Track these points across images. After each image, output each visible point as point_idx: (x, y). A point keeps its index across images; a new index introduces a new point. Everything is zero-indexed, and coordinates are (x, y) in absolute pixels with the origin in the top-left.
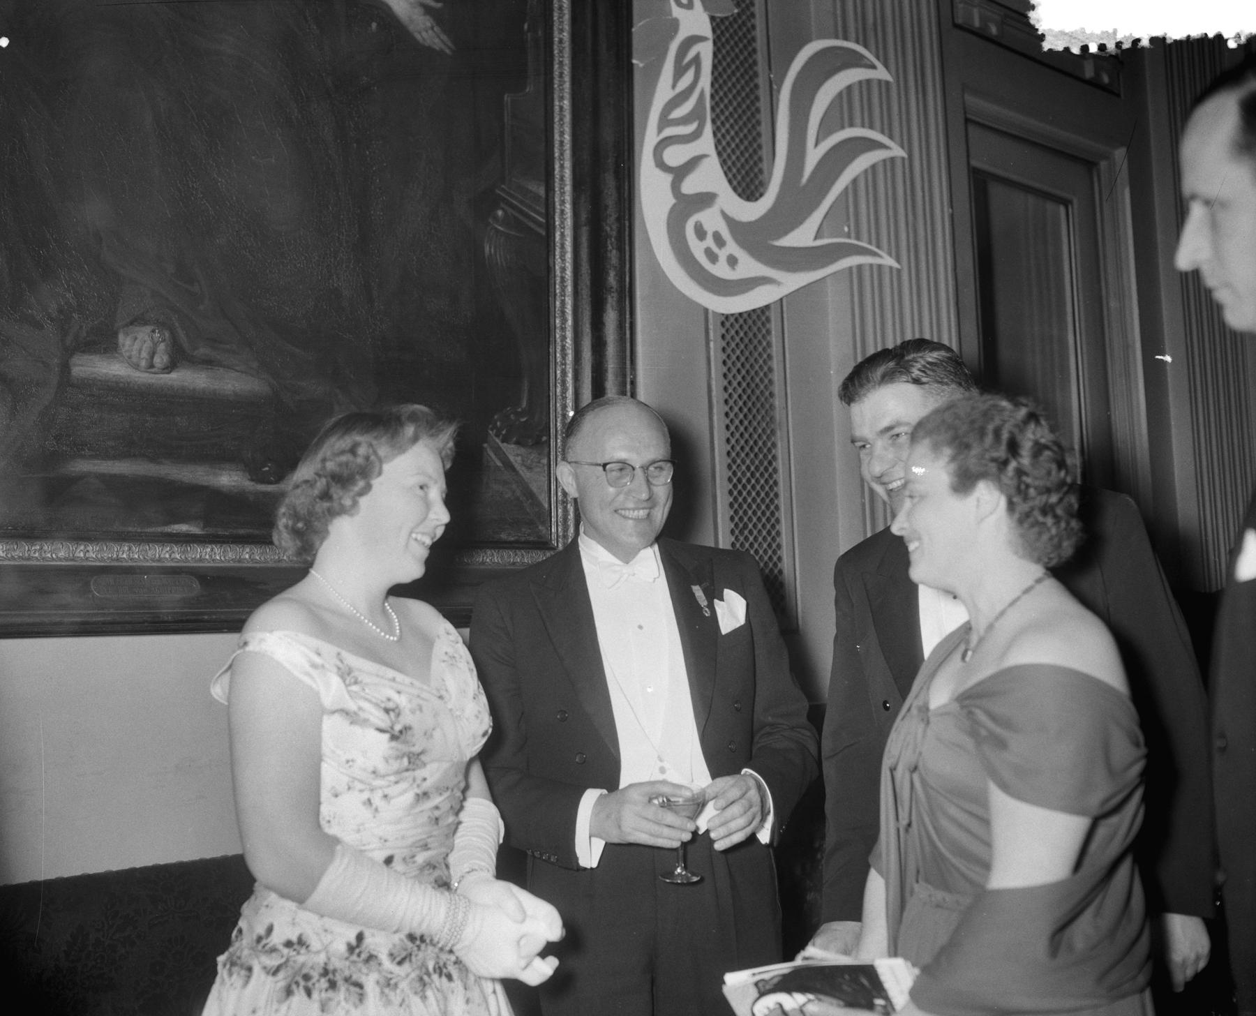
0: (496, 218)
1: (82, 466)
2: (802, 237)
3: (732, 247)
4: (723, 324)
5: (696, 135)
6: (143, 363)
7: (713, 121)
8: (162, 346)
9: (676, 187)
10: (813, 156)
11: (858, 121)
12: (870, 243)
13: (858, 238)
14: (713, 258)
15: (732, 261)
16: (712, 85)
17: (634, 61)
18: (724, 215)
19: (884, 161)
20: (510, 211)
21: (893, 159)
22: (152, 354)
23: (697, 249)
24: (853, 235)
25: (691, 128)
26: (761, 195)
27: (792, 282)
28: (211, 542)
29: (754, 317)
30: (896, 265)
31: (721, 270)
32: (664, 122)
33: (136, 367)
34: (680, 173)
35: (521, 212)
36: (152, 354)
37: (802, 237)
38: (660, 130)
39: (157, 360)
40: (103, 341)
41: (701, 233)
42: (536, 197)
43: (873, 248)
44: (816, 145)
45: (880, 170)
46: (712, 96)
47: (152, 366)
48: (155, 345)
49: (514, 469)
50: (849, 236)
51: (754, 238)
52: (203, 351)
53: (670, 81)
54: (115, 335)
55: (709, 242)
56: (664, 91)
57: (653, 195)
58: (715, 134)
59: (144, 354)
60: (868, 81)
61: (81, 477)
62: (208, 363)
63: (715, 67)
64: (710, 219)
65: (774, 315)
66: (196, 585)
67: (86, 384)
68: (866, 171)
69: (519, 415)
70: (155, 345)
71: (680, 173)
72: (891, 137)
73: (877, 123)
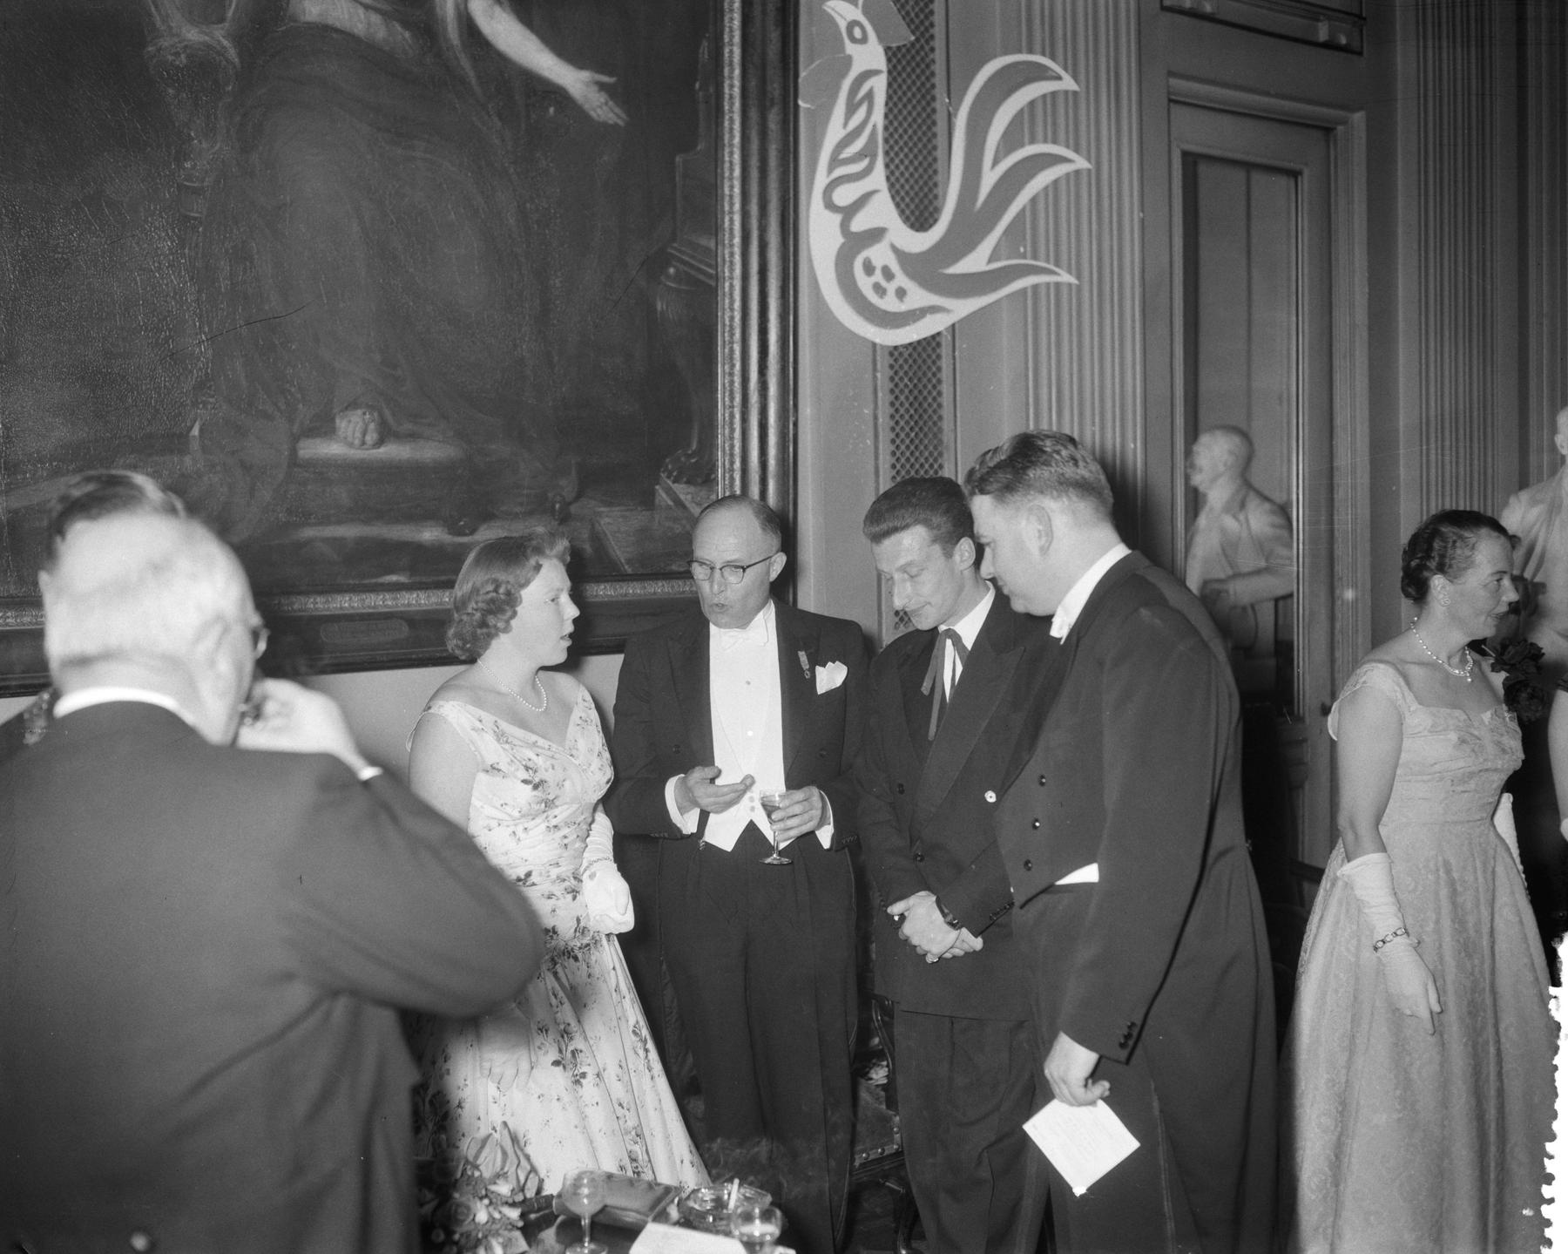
0: (668, 276)
1: (309, 533)
2: (976, 261)
3: (901, 280)
4: (891, 354)
5: (867, 171)
6: (357, 442)
7: (887, 153)
8: (372, 426)
9: (845, 226)
10: (989, 178)
11: (1040, 135)
12: (1048, 261)
13: (1035, 257)
14: (879, 290)
15: (901, 293)
16: (886, 116)
17: (800, 103)
18: (894, 249)
19: (1068, 175)
20: (682, 267)
21: (1077, 172)
22: (364, 434)
23: (865, 283)
24: (1029, 254)
25: (865, 163)
26: (936, 221)
27: (962, 308)
28: (420, 589)
29: (929, 343)
30: (1073, 280)
31: (890, 304)
32: (835, 162)
33: (351, 445)
34: (849, 212)
35: (692, 266)
36: (364, 434)
37: (976, 261)
38: (830, 170)
39: (368, 438)
40: (323, 426)
41: (869, 269)
42: (707, 250)
43: (1052, 267)
44: (995, 162)
45: (1063, 187)
46: (886, 128)
47: (363, 443)
48: (366, 426)
49: (684, 507)
50: (1024, 256)
51: (924, 269)
52: (408, 426)
53: (842, 120)
54: (333, 420)
55: (878, 277)
56: (835, 131)
57: (821, 236)
58: (887, 166)
59: (358, 434)
60: (1054, 94)
61: (309, 542)
62: (412, 436)
63: (889, 98)
64: (880, 254)
65: (946, 341)
66: (405, 629)
67: (310, 464)
68: (1046, 188)
69: (690, 456)
70: (366, 426)
71: (849, 212)
72: (1077, 151)
73: (1062, 135)
